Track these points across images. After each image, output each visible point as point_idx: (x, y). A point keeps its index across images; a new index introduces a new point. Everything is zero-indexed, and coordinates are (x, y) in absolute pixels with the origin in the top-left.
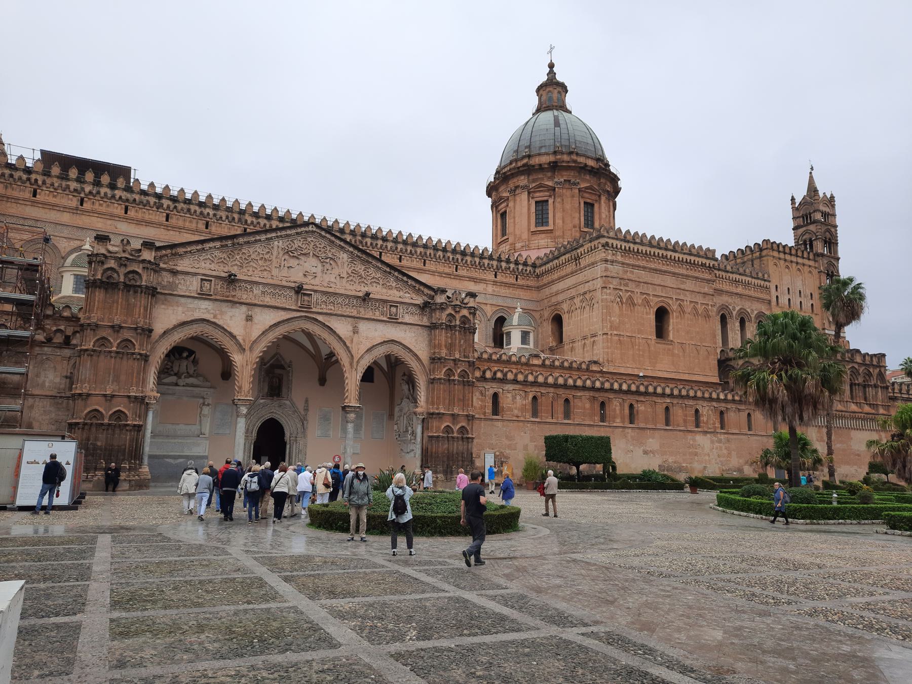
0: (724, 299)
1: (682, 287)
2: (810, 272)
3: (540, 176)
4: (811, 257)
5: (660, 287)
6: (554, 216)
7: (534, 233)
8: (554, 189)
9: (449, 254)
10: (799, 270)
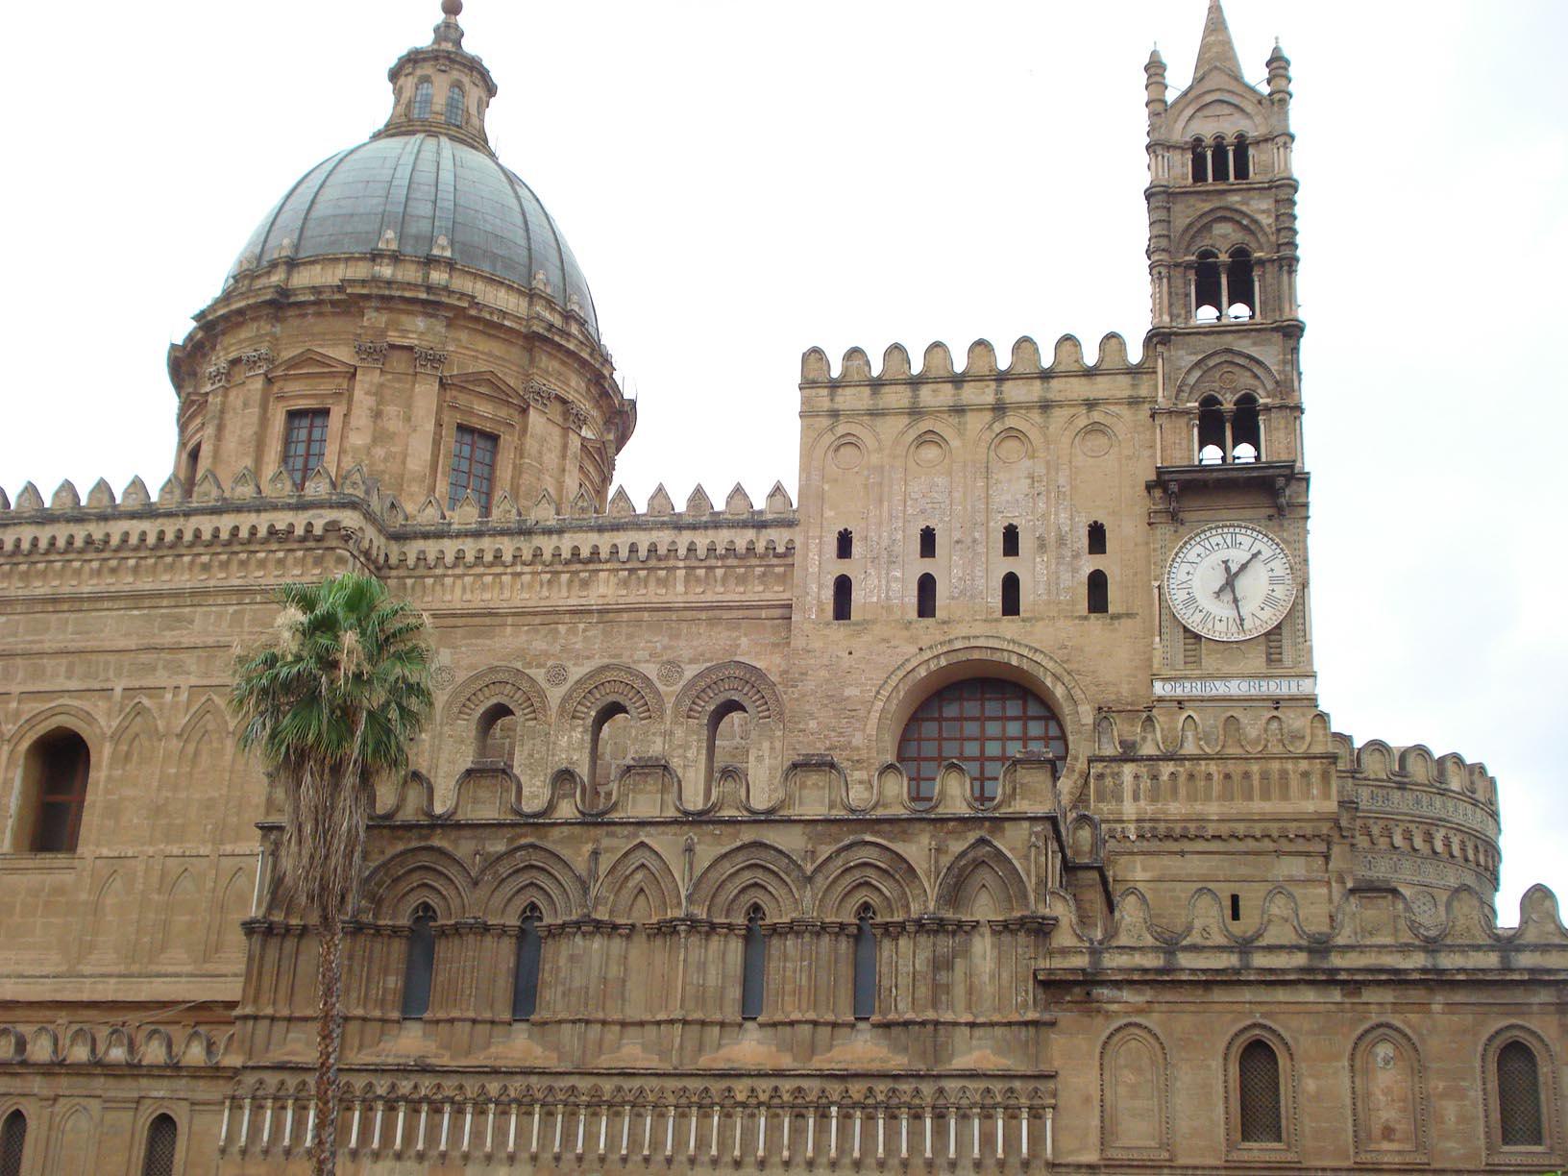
0: (508, 642)
1: (168, 638)
5: (64, 661)
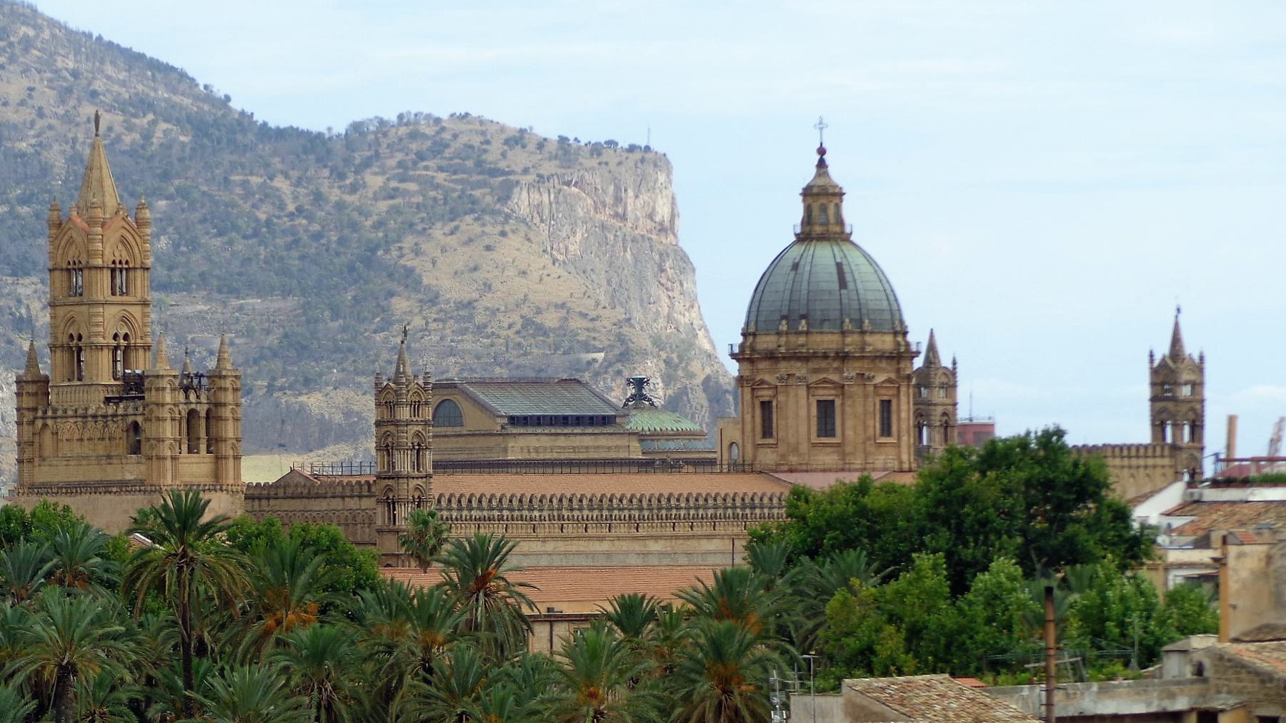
2: (1164, 475)
3: (824, 364)
4: (1167, 452)
6: (843, 424)
7: (814, 445)
8: (843, 386)
9: (738, 511)
10: (1148, 475)
